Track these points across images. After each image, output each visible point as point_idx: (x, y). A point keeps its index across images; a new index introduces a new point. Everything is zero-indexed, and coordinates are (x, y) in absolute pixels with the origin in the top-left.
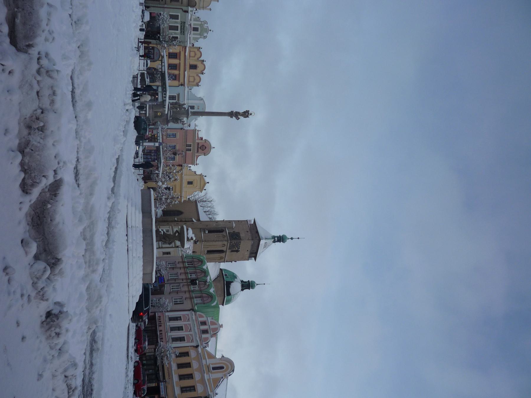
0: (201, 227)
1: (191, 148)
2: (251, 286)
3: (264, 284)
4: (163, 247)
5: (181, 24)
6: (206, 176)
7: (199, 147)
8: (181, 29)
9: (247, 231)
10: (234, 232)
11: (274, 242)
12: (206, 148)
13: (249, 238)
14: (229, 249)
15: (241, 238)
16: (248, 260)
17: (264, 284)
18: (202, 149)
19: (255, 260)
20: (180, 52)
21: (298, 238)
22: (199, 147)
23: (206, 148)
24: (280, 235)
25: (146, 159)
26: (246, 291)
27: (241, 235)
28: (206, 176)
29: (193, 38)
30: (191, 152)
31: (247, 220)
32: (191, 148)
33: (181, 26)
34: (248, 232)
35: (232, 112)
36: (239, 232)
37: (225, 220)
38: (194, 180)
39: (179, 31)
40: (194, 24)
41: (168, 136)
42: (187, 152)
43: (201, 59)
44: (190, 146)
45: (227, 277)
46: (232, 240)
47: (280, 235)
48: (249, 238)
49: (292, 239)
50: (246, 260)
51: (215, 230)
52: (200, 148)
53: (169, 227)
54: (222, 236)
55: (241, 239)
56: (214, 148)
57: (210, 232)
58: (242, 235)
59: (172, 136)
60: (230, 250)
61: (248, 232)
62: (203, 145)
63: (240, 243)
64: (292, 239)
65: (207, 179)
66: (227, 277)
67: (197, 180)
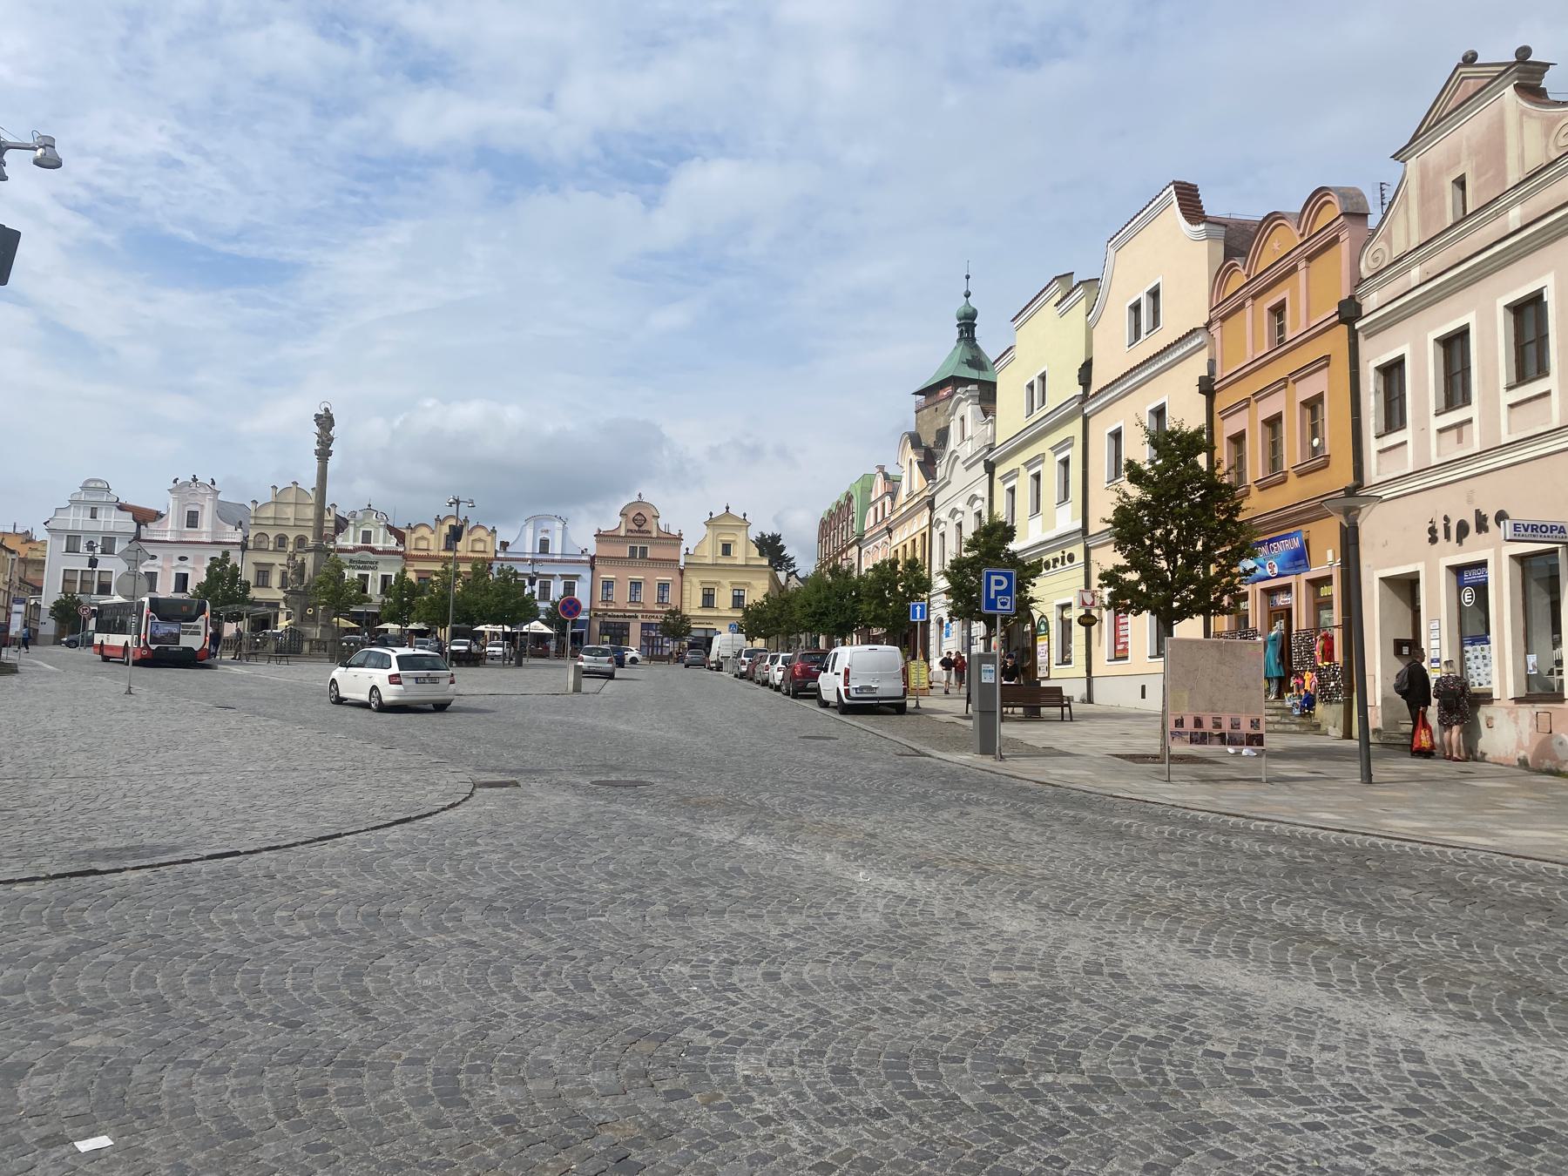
1: (638, 546)
5: (353, 568)
6: (711, 514)
7: (637, 528)
8: (365, 568)
12: (639, 514)
20: (415, 571)
21: (968, 277)
22: (637, 528)
23: (639, 514)
24: (958, 326)
28: (711, 514)
29: (385, 542)
31: (917, 412)
33: (359, 568)
35: (317, 452)
39: (370, 573)
40: (355, 541)
41: (610, 599)
43: (432, 524)
44: (633, 549)
47: (958, 326)
52: (640, 526)
56: (640, 495)
59: (610, 590)
62: (634, 520)
64: (967, 295)
65: (719, 511)
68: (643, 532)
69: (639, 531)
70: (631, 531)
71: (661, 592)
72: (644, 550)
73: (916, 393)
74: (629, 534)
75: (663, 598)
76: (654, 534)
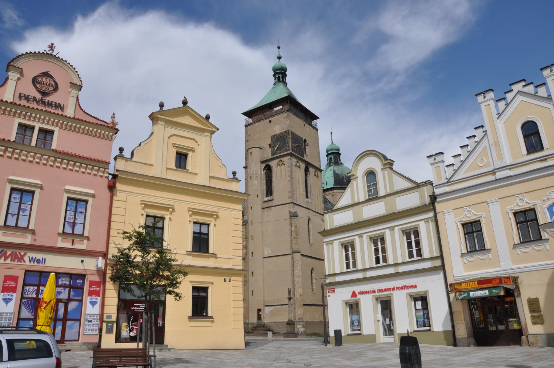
0: (260, 208)
1: (38, 126)
2: (337, 151)
3: (331, 133)
4: (436, 253)
7: (38, 96)
9: (269, 122)
10: (270, 145)
11: (285, 84)
12: (46, 74)
13: (285, 118)
14: (304, 158)
15: (284, 131)
16: (317, 130)
17: (331, 133)
18: (51, 89)
19: (317, 118)
25: (69, 323)
26: (343, 159)
27: (278, 133)
28: (162, 105)
30: (56, 130)
31: (246, 126)
32: (38, 126)
34: (270, 122)
36: (271, 136)
37: (244, 166)
38: (175, 146)
42: (54, 147)
45: (327, 184)
46: (289, 147)
48: (285, 118)
49: (279, 58)
50: (318, 133)
51: (265, 181)
52: (44, 94)
53: (332, 242)
54: (279, 167)
55: (286, 132)
57: (269, 191)
58: (278, 129)
60: (305, 155)
61: (270, 122)
62: (35, 81)
63: (294, 133)
64: (279, 58)
66: (327, 184)
67: (174, 135)
68: (50, 104)
69: (43, 103)
70: (27, 98)
71: (70, 214)
72: (46, 134)
73: (245, 114)
74: (24, 102)
75: (74, 225)
76: (70, 112)
